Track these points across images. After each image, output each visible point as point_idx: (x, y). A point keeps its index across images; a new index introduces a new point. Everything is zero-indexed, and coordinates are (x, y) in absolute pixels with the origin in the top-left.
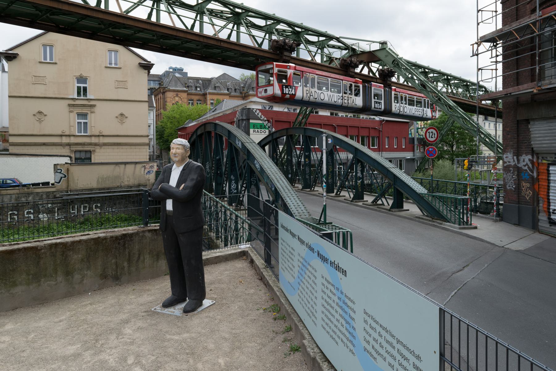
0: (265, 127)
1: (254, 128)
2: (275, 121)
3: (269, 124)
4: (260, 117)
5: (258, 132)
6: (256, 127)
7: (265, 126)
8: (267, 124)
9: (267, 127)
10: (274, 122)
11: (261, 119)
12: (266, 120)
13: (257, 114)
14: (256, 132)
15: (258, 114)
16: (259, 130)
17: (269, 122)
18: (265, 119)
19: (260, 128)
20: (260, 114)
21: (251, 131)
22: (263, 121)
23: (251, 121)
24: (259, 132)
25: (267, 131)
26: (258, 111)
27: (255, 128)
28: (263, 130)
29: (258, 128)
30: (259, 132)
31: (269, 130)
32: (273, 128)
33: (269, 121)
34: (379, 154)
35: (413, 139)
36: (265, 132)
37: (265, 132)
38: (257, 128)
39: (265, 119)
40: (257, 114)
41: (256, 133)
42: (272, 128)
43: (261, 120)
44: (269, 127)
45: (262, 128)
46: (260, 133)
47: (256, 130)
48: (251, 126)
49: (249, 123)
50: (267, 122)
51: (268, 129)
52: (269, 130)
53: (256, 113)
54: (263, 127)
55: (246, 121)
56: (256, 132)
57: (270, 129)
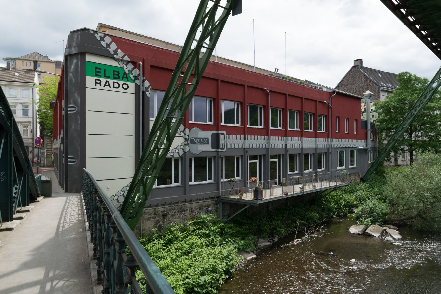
0: (125, 77)
1: (96, 75)
2: (151, 66)
3: (136, 72)
4: (113, 53)
5: (107, 84)
6: (102, 73)
7: (125, 73)
8: (131, 71)
9: (132, 76)
10: (148, 68)
11: (115, 56)
12: (128, 62)
13: (105, 46)
14: (103, 84)
15: (108, 45)
16: (111, 81)
17: (135, 67)
18: (126, 58)
19: (114, 78)
20: (114, 46)
21: (90, 81)
22: (121, 64)
23: (89, 58)
24: (111, 85)
25: (132, 86)
26: (108, 40)
27: (100, 76)
28: (121, 83)
29: (109, 77)
30: (111, 85)
31: (136, 84)
32: (146, 82)
33: (135, 65)
34: (315, 141)
35: (366, 122)
36: (125, 86)
37: (125, 86)
38: (105, 77)
39: (126, 58)
40: (105, 46)
41: (102, 87)
42: (144, 81)
43: (117, 60)
44: (136, 78)
45: (118, 78)
46: (112, 89)
47: (104, 80)
48: (89, 69)
49: (83, 61)
50: (130, 66)
51: (133, 81)
52: (136, 84)
53: (103, 43)
54: (121, 75)
55: (77, 59)
56: (103, 84)
57: (137, 82)
